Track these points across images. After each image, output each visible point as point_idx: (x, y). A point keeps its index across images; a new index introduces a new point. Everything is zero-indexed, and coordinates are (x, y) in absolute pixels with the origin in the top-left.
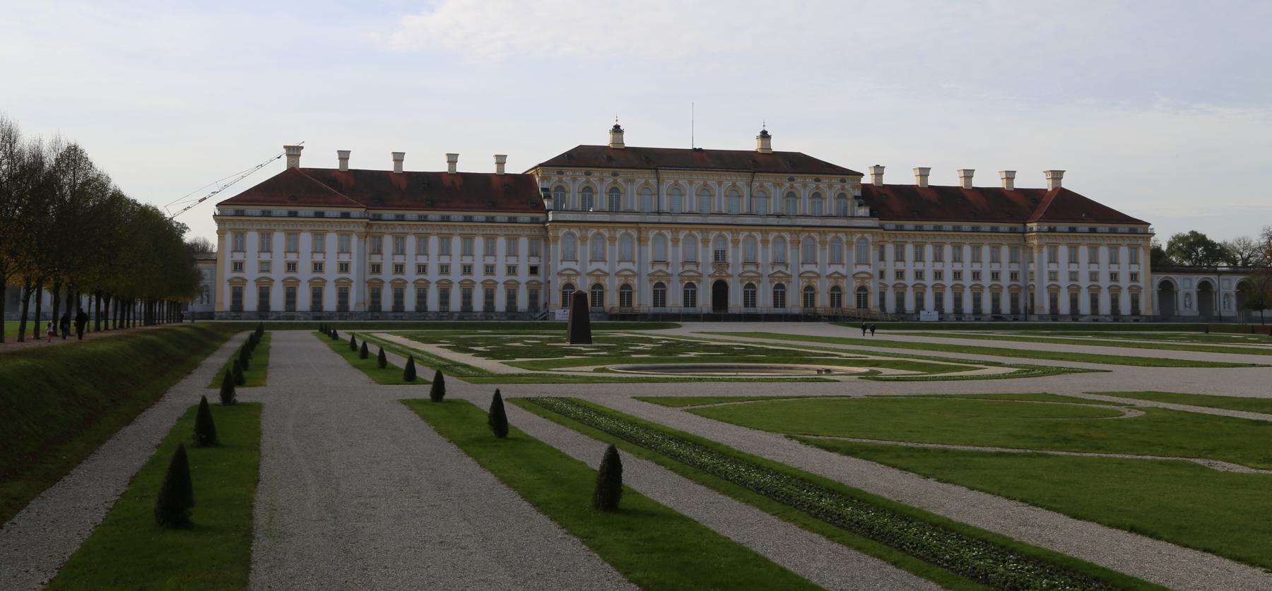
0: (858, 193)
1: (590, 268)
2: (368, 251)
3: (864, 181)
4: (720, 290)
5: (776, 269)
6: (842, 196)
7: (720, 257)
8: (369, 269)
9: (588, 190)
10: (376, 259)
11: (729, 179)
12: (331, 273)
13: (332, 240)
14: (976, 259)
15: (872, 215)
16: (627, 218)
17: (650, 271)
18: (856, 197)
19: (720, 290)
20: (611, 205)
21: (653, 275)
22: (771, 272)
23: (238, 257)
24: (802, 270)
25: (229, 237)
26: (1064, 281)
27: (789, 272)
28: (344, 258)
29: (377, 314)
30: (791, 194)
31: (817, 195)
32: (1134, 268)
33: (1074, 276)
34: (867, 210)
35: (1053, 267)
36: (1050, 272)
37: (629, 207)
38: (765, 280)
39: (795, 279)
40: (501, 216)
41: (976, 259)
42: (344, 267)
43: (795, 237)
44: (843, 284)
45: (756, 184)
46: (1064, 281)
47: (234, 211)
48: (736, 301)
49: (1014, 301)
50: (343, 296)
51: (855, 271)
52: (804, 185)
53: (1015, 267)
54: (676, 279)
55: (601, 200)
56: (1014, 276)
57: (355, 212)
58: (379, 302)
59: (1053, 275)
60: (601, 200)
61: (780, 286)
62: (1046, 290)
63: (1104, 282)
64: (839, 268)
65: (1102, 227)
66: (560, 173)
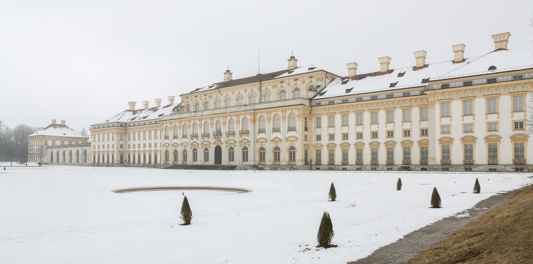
5: (243, 138)
7: (218, 134)
14: (390, 120)
24: (258, 137)
26: (457, 133)
27: (249, 139)
33: (468, 128)
36: (442, 127)
39: (252, 144)
41: (390, 120)
44: (281, 145)
46: (457, 133)
47: (95, 128)
51: (287, 136)
53: (424, 125)
59: (445, 129)
61: (245, 148)
62: (437, 143)
64: (277, 135)
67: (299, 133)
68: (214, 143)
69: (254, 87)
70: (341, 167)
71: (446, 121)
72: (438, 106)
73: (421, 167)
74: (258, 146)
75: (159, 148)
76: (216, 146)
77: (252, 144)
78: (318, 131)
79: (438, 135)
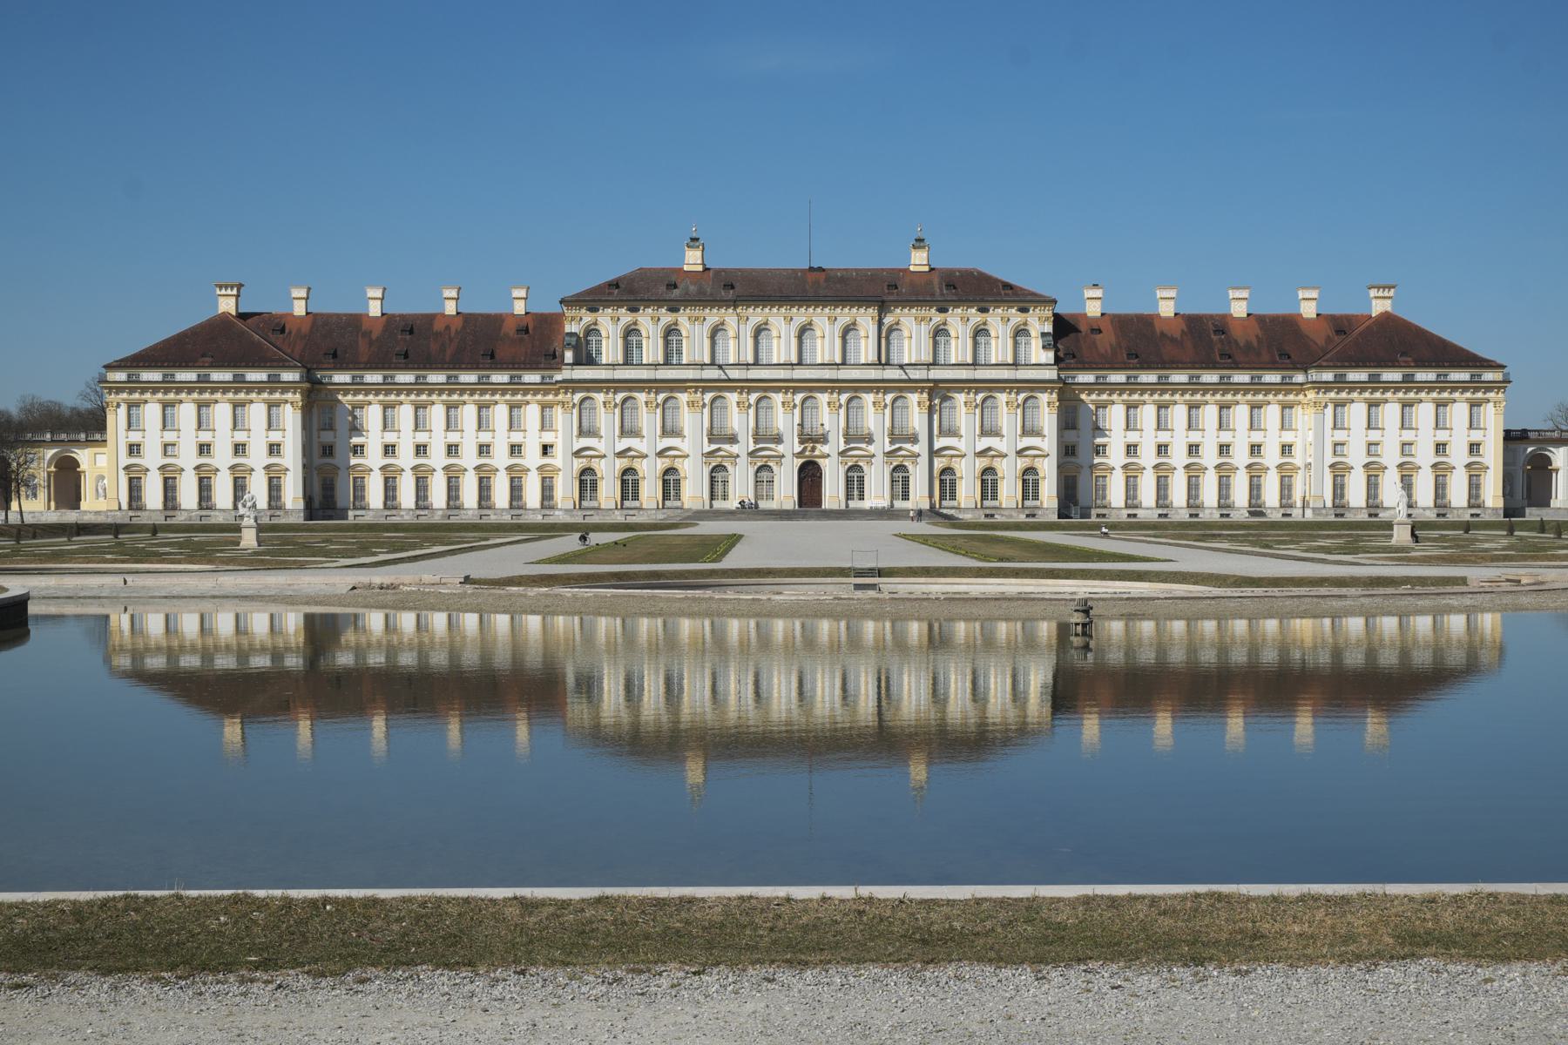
0: (1048, 328)
1: (620, 447)
2: (315, 426)
3: (1059, 310)
4: (810, 476)
6: (1020, 332)
8: (317, 451)
9: (630, 332)
10: (327, 437)
11: (845, 315)
12: (257, 457)
13: (257, 412)
15: (1058, 360)
16: (690, 374)
17: (708, 448)
18: (1043, 335)
19: (810, 476)
20: (667, 355)
21: (711, 454)
22: (888, 448)
23: (135, 437)
24: (936, 447)
25: (123, 410)
26: (1356, 456)
27: (916, 449)
28: (275, 437)
29: (330, 512)
30: (939, 332)
31: (980, 332)
32: (1476, 436)
34: (1051, 354)
35: (1340, 436)
37: (698, 359)
38: (879, 460)
40: (500, 377)
42: (274, 449)
43: (925, 395)
45: (888, 320)
46: (1356, 456)
48: (833, 492)
49: (1286, 489)
50: (274, 489)
51: (1020, 446)
52: (960, 322)
53: (1288, 437)
54: (743, 460)
55: (651, 350)
56: (1286, 449)
57: (288, 376)
58: (332, 497)
60: (651, 350)
62: (1327, 470)
63: (1425, 456)
65: (1423, 375)
66: (593, 310)
67: (1048, 442)
68: (799, 455)
69: (866, 319)
70: (1126, 512)
71: (1340, 436)
72: (1330, 410)
73: (1282, 511)
74: (939, 464)
75: (558, 459)
76: (801, 461)
77: (924, 460)
78: (1071, 436)
79: (1330, 459)
